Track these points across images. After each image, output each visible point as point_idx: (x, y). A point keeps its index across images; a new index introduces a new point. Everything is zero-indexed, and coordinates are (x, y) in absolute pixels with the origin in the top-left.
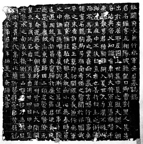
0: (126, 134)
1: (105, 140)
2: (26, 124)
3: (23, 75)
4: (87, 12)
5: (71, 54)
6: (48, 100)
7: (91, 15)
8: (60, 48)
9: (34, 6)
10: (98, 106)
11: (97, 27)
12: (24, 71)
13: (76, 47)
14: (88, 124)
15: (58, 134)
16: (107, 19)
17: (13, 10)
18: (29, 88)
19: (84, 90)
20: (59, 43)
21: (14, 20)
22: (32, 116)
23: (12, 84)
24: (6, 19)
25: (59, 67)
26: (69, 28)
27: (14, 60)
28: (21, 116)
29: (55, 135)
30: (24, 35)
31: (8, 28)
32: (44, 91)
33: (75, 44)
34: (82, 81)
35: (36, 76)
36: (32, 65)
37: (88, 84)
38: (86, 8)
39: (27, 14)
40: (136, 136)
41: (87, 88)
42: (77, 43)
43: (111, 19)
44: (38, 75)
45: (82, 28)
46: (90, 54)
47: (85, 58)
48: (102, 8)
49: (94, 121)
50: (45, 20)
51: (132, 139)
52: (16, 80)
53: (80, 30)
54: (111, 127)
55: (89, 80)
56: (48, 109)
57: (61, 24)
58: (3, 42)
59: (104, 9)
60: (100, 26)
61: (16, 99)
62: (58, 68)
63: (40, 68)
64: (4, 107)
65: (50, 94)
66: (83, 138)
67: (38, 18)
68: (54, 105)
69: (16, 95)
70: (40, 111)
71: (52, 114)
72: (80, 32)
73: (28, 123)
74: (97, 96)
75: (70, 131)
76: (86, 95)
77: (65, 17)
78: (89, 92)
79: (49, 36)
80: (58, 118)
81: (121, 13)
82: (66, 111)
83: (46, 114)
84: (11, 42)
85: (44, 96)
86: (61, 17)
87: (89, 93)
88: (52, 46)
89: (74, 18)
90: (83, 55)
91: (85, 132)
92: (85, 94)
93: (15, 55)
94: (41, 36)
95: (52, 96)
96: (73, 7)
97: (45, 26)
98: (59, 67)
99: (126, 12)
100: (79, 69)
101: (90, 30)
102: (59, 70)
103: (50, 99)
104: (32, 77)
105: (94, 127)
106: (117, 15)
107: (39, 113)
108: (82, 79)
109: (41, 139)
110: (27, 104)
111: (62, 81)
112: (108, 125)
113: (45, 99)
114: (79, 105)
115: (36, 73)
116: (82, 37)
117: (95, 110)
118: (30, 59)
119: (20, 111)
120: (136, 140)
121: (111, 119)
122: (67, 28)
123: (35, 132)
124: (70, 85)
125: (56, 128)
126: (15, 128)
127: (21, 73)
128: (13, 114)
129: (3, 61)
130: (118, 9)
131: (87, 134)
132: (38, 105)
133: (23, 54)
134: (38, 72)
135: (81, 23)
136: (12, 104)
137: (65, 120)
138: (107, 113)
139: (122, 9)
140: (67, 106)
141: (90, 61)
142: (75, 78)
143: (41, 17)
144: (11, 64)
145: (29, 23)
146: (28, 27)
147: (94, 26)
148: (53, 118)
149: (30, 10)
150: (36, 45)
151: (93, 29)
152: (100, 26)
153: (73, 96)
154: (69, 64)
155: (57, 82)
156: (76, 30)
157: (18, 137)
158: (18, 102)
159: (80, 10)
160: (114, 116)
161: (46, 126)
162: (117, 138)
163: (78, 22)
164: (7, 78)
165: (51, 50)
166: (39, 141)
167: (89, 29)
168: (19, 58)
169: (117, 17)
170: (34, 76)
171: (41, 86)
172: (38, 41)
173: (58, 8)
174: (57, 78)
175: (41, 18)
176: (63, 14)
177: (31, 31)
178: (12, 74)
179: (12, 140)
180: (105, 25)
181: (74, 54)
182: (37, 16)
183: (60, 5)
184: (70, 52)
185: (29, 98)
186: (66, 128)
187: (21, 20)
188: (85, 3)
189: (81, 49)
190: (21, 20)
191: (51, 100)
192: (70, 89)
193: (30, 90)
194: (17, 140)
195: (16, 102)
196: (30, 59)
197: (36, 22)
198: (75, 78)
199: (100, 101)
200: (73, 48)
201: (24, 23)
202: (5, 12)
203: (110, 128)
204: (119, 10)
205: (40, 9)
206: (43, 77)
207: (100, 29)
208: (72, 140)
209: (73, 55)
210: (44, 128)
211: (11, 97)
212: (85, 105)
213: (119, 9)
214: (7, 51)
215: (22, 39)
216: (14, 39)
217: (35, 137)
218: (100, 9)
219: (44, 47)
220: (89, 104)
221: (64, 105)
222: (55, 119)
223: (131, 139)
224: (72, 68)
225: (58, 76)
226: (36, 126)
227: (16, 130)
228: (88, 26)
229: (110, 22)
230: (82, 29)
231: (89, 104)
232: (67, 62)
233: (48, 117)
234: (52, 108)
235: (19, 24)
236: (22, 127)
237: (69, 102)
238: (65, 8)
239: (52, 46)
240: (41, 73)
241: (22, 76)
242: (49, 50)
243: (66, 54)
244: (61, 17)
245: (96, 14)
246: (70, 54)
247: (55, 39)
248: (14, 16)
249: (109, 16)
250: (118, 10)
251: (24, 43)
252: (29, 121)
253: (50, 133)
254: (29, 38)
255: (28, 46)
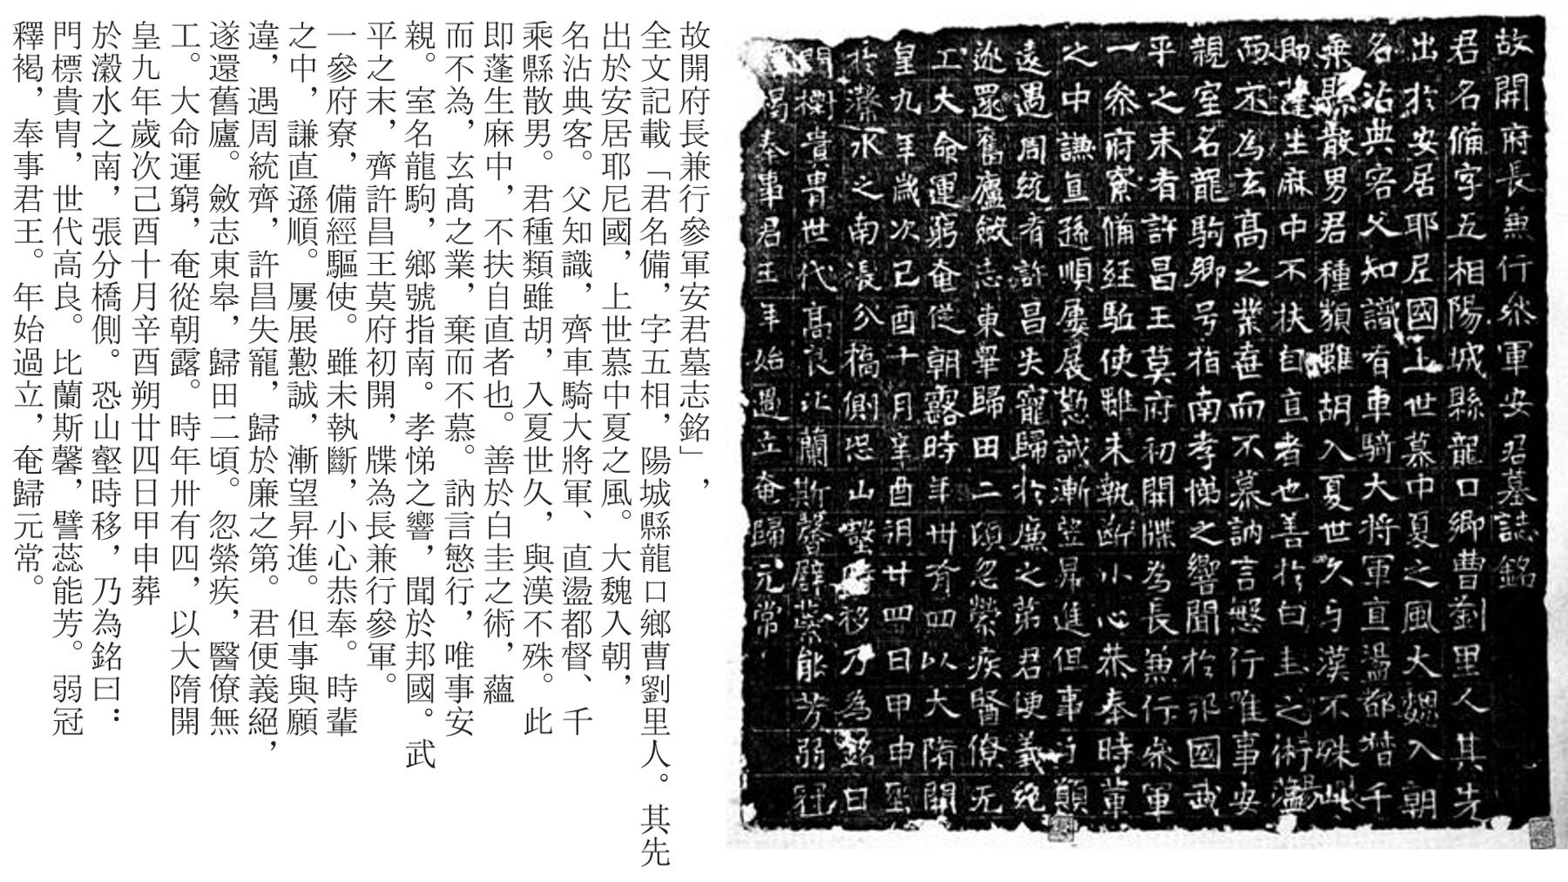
0: (1465, 789)
1: (1343, 825)
2: (882, 729)
3: (863, 440)
4: (1240, 72)
5: (1142, 317)
6: (1009, 591)
7: (1261, 87)
8: (1079, 283)
9: (928, 37)
10: (1301, 623)
11: (1299, 161)
12: (869, 421)
13: (1173, 275)
14: (1245, 734)
15: (1066, 788)
16: (1354, 109)
17: (801, 59)
18: (894, 518)
19: (1222, 532)
20: (1073, 253)
21: (808, 117)
22: (916, 683)
23: (795, 495)
24: (761, 112)
25: (1075, 396)
26: (1132, 163)
27: (807, 351)
28: (852, 682)
29: (1047, 798)
30: (865, 205)
31: (774, 167)
32: (984, 539)
33: (1167, 258)
34: (1207, 475)
35: (940, 451)
36: (913, 385)
37: (1246, 494)
38: (1234, 50)
39: (886, 83)
40: (1518, 791)
41: (1237, 519)
42: (1181, 250)
43: (1380, 109)
44: (950, 441)
45: (1209, 163)
46: (1258, 320)
47: (1226, 342)
48: (1325, 49)
49: (1279, 714)
50: (989, 115)
51: (1501, 822)
52: (820, 475)
53: (1200, 175)
54: (1380, 749)
55: (1251, 474)
56: (1008, 644)
57: (1084, 144)
58: (742, 249)
59: (1336, 55)
60: (1312, 156)
61: (821, 586)
62: (1067, 400)
63: (964, 404)
64: (749, 632)
65: (1023, 555)
66: (1216, 812)
67: (948, 104)
68: (1047, 621)
69: (817, 563)
70: (960, 654)
71: (1033, 672)
72: (1198, 187)
73: (891, 726)
74: (1294, 567)
75: (1138, 770)
76: (1234, 562)
77: (1107, 97)
78: (1251, 540)
79: (1016, 213)
80: (1069, 694)
81: (1438, 80)
82: (1113, 653)
83: (998, 675)
84: (790, 250)
85: (985, 569)
86: (1086, 101)
87: (1248, 548)
88: (1031, 271)
89: (1164, 106)
90: (1213, 322)
91: (1227, 779)
92: (1224, 553)
93: (815, 323)
94: (967, 215)
95: (1031, 568)
96: (1157, 43)
97: (989, 151)
98: (1075, 396)
99: (1468, 72)
100: (1191, 405)
101: (1255, 178)
102: (1072, 414)
103: (1021, 582)
104: (913, 453)
105: (1283, 751)
106: (1416, 89)
107: (953, 667)
108: (1207, 467)
109: (969, 818)
110: (885, 612)
111: (1094, 480)
112: (1365, 739)
113: (990, 583)
114: (1193, 621)
115: (939, 434)
116: (1207, 221)
117: (1287, 650)
118: (904, 349)
119: (847, 653)
120: (1526, 827)
121: (1378, 703)
122: (1119, 168)
123: (931, 779)
124: (1139, 501)
125: (1054, 757)
126: (812, 754)
127: (852, 433)
128: (800, 674)
129: (744, 360)
130: (1419, 54)
131: (1240, 789)
132: (948, 620)
133: (864, 316)
134: (947, 423)
135: (1205, 135)
136: (798, 613)
137: (1106, 708)
138: (1356, 664)
139: (1445, 52)
140: (1120, 625)
141: (1254, 358)
142: (1166, 457)
143: (966, 98)
144: (790, 380)
145: (900, 137)
146: (894, 161)
147: (1279, 152)
148: (1036, 698)
149: (904, 61)
150: (940, 264)
151: (1271, 172)
152: (1312, 156)
153: (1155, 567)
154: (1130, 375)
155: (1060, 485)
156: (1176, 178)
157: (833, 806)
158: (829, 601)
159: (1199, 58)
160: (1395, 684)
161: (995, 745)
162: (1413, 812)
163: (1185, 132)
164: (770, 462)
165: (1027, 295)
166: (954, 833)
167: (1250, 173)
168: (837, 344)
169: (1415, 100)
170: (927, 447)
171: (964, 508)
172: (949, 240)
173: (1065, 49)
174: (1063, 459)
175: (967, 107)
176: (1097, 83)
177: (910, 185)
178: (797, 434)
179: (797, 825)
180: (1344, 148)
181: (1160, 318)
182: (943, 96)
183: (1079, 27)
184: (1139, 306)
185: (898, 576)
186: (1113, 753)
187: (849, 116)
188: (1226, 19)
189: (1204, 289)
190: (849, 116)
191: (1027, 590)
192: (1138, 525)
193: (902, 528)
194: (829, 827)
195: (822, 604)
196: (904, 349)
197: (936, 132)
198: (1169, 462)
199: (1315, 595)
200: (1156, 280)
201: (865, 137)
202: (754, 71)
203: (1372, 754)
204: (1424, 56)
205: (964, 51)
206: (977, 455)
207: (1312, 170)
208: (1148, 824)
209: (1155, 322)
210: (983, 752)
211: (790, 569)
212: (1227, 622)
213: (1429, 53)
214: (767, 302)
215: (855, 229)
216: (806, 228)
217: (934, 807)
218: (1312, 54)
219: (984, 277)
220: (1249, 614)
221: (1105, 621)
222: (1051, 703)
223: (1496, 821)
224: (1150, 403)
225: (1066, 448)
226: (936, 745)
227: (822, 767)
228: (1242, 151)
229: (1376, 128)
230: (1209, 171)
231: (1249, 614)
232: (1119, 367)
233: (1008, 688)
234: (1030, 638)
235: (836, 141)
236: (858, 752)
237: (1134, 599)
238: (1110, 49)
239: (1031, 271)
240: (967, 430)
241: (856, 449)
242: (1013, 295)
243: (1115, 317)
244: (1086, 101)
245: (1293, 81)
246: (1140, 318)
247: (1051, 230)
248: (809, 94)
249: (1367, 94)
250: (1419, 60)
251: (866, 251)
252: (895, 714)
253: (1022, 787)
254: (894, 223)
255: (893, 271)
